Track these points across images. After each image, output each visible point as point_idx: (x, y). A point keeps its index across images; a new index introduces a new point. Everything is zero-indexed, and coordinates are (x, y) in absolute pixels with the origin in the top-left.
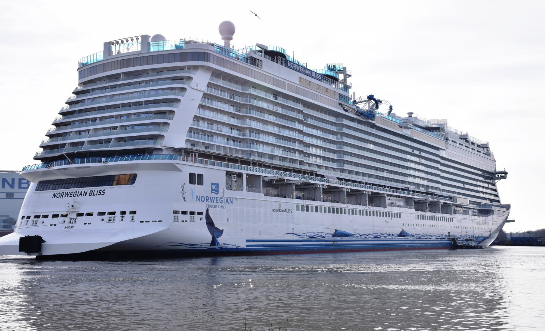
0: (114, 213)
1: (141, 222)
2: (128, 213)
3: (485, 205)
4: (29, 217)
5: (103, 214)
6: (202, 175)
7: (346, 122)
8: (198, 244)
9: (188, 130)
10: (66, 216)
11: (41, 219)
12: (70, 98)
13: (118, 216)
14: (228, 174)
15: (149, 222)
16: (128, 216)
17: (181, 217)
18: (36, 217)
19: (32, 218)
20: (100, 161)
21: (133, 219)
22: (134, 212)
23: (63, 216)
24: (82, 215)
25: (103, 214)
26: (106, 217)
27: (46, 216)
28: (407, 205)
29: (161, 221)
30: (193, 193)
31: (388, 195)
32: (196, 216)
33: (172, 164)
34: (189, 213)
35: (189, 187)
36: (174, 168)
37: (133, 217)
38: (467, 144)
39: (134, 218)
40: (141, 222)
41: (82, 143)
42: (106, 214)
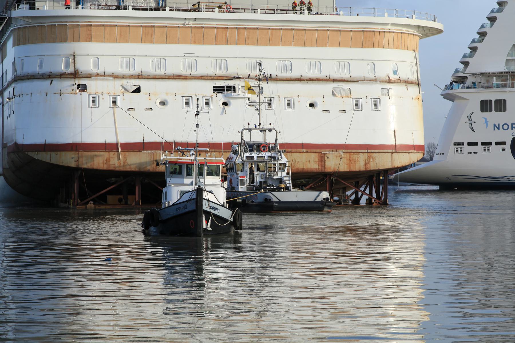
6: (505, 101)
8: (502, 177)
17: (466, 148)
29: (469, 153)
30: (486, 122)
32: (466, 148)
34: (480, 144)
35: (479, 116)
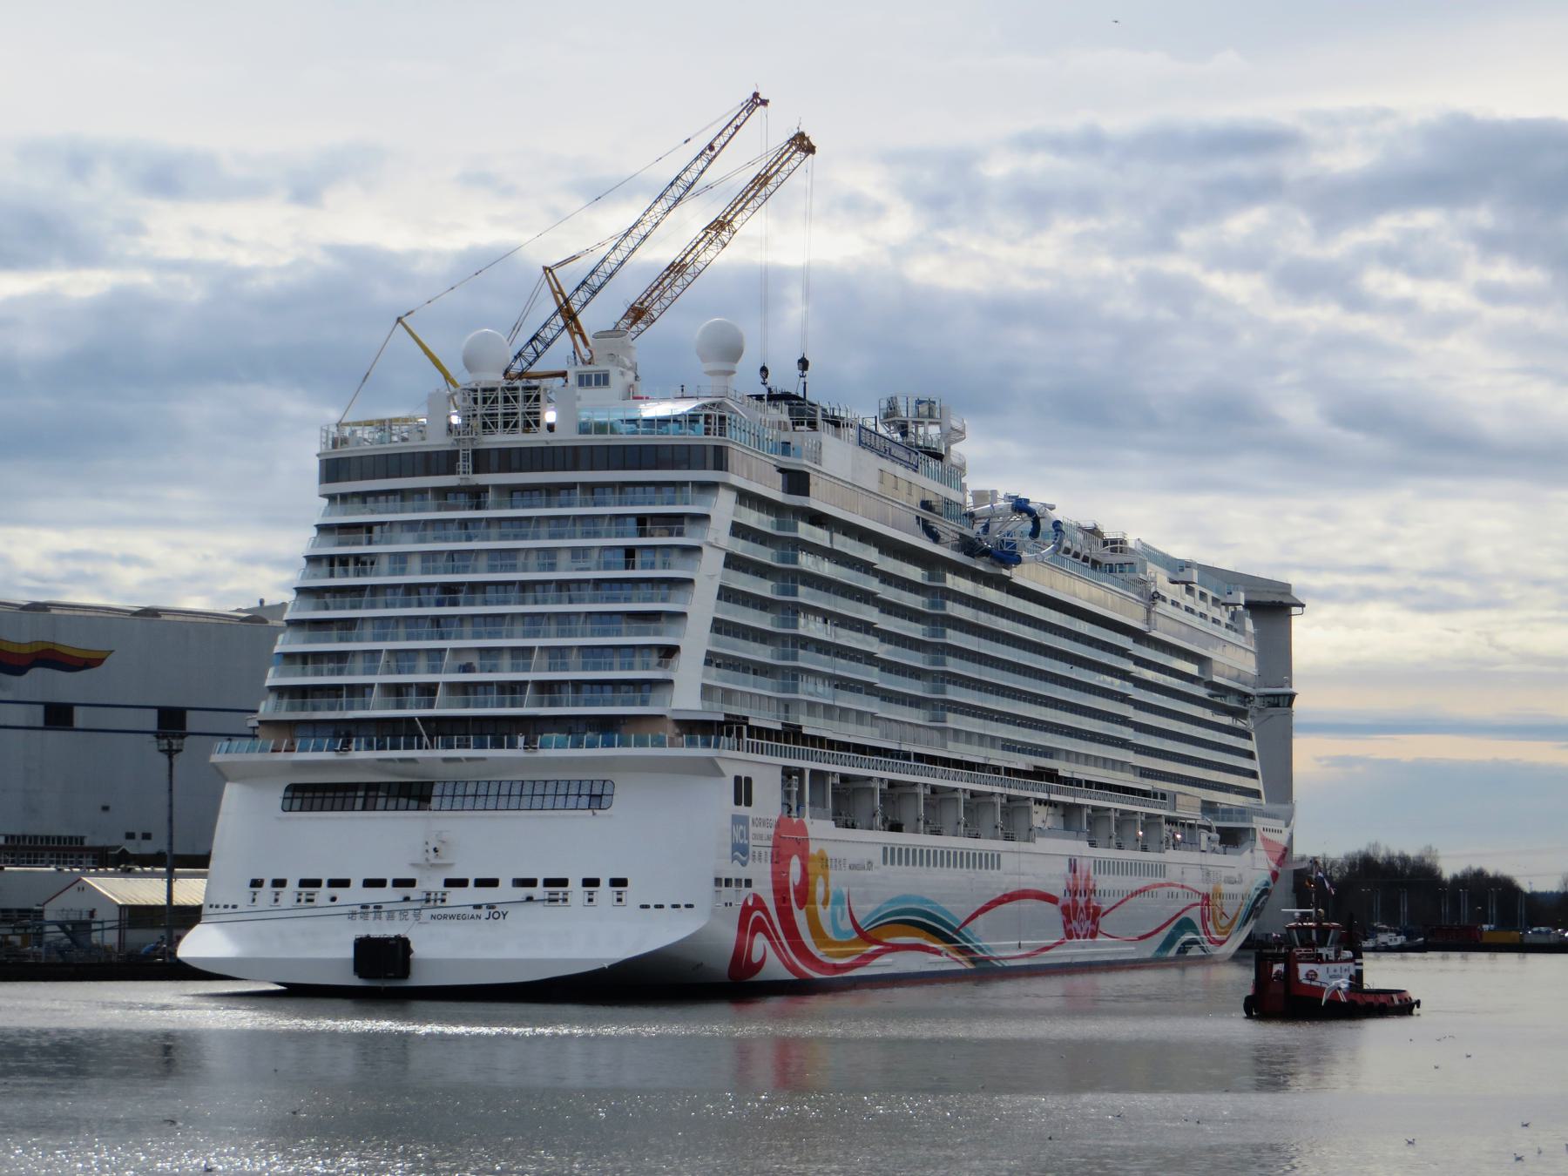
0: (563, 882)
1: (643, 907)
2: (605, 883)
3: (1229, 812)
4: (279, 883)
5: (531, 883)
7: (954, 582)
9: (703, 657)
10: (410, 883)
11: (324, 893)
12: (1376, 845)
13: (576, 889)
14: (788, 773)
15: (661, 906)
16: (605, 892)
18: (304, 883)
19: (292, 885)
20: (512, 745)
21: (619, 900)
22: (618, 883)
23: (398, 883)
24: (462, 883)
25: (531, 883)
26: (539, 891)
27: (345, 883)
28: (1067, 827)
31: (1039, 802)
33: (711, 760)
36: (712, 769)
37: (619, 893)
38: (1188, 600)
39: (623, 897)
40: (643, 907)
41: (428, 690)
42: (540, 883)
